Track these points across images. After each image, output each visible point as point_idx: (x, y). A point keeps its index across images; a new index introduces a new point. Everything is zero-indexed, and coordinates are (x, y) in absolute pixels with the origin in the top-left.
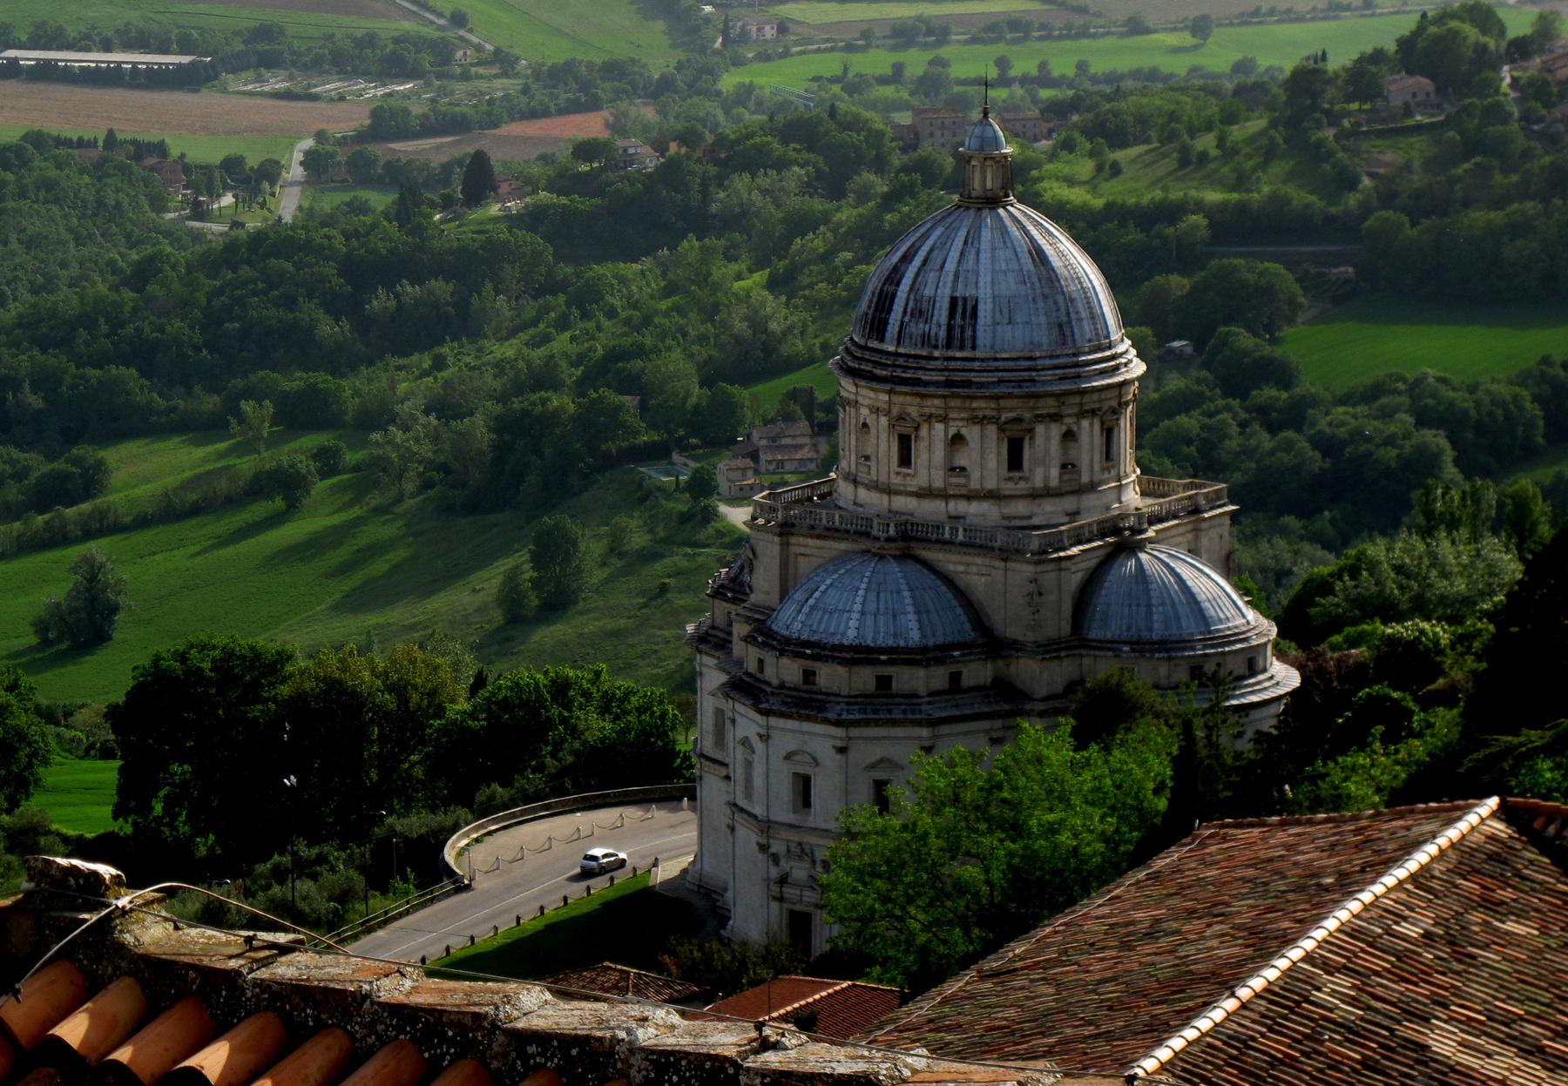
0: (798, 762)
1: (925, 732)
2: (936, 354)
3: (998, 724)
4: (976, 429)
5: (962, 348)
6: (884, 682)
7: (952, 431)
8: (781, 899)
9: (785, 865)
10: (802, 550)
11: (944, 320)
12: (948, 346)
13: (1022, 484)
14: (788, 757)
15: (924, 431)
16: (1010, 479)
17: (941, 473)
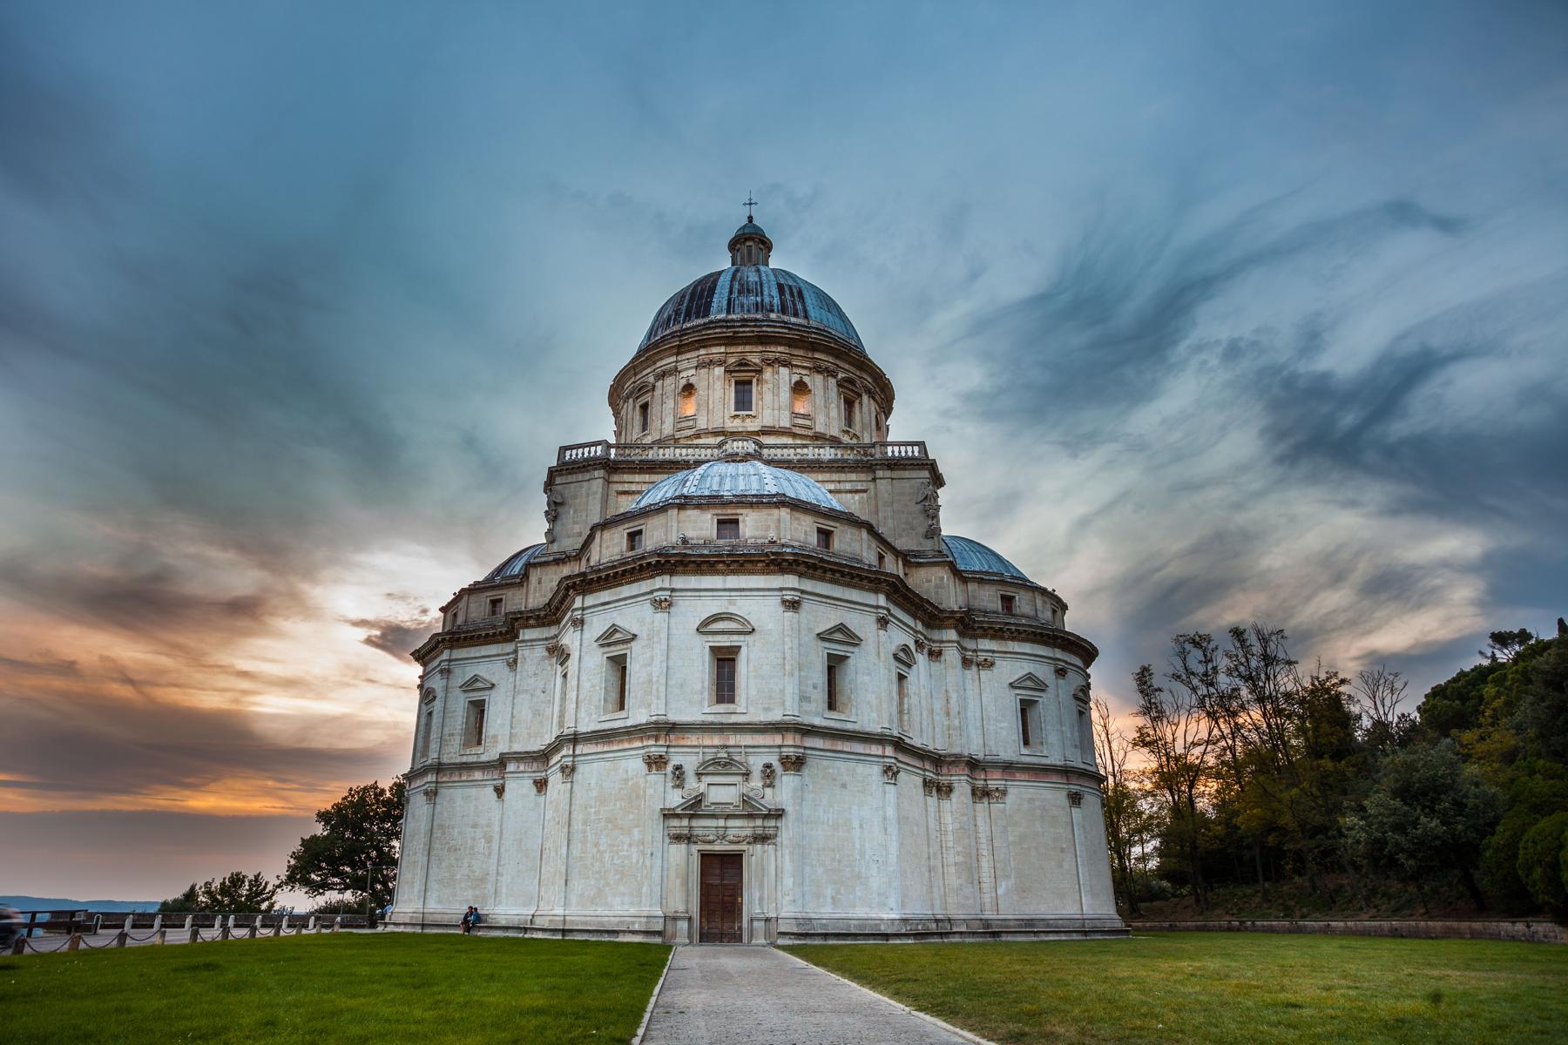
1: (882, 600)
2: (773, 316)
3: (920, 627)
4: (819, 378)
5: (796, 315)
6: (825, 535)
7: (795, 378)
8: (688, 839)
9: (693, 785)
10: (626, 487)
11: (775, 292)
12: (784, 310)
14: (703, 628)
15: (768, 374)
17: (787, 413)
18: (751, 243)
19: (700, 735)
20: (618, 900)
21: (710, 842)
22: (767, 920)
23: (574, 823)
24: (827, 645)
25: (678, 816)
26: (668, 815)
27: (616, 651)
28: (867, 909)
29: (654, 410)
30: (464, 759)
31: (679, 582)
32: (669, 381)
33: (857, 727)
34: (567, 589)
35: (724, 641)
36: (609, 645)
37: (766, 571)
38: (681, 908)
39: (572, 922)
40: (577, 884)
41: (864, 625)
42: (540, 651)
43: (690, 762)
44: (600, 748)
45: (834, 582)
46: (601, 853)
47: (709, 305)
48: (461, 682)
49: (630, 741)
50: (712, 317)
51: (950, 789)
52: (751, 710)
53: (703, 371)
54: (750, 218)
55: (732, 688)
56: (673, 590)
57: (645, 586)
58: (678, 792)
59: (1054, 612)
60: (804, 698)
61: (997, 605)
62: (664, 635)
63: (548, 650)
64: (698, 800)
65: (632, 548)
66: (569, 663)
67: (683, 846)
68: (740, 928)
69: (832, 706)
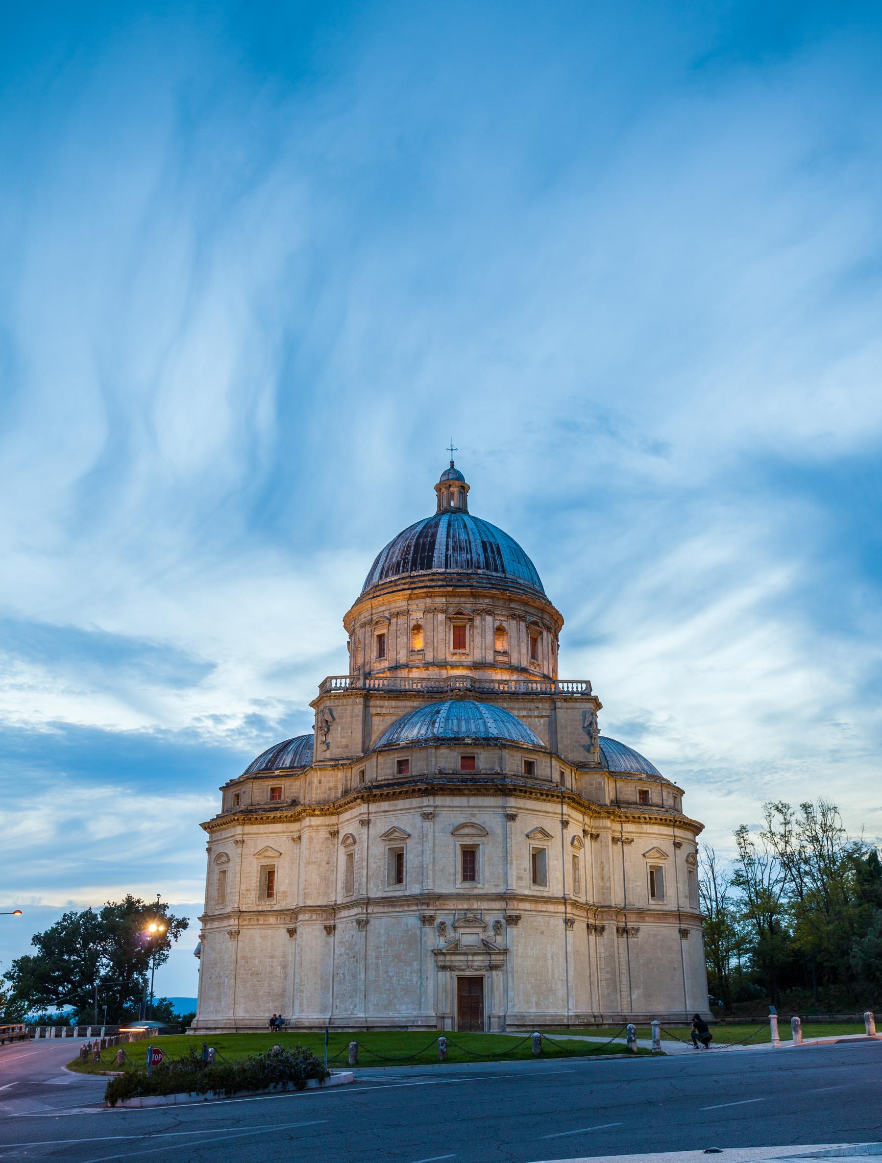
0: (468, 835)
2: (480, 571)
3: (587, 820)
5: (496, 570)
6: (530, 766)
7: (497, 623)
8: (451, 968)
10: (378, 710)
11: (480, 550)
12: (487, 567)
13: (537, 669)
15: (477, 621)
16: (533, 664)
18: (453, 485)
19: (455, 902)
20: (404, 1007)
21: (463, 970)
22: (499, 1017)
23: (369, 958)
24: (532, 842)
25: (444, 954)
26: (437, 953)
27: (396, 845)
28: (555, 1010)
29: (389, 643)
30: (260, 909)
31: (439, 800)
32: (402, 620)
33: (549, 894)
34: (355, 799)
35: (469, 841)
36: (390, 840)
37: (495, 795)
38: (448, 1011)
39: (372, 1022)
40: (373, 998)
41: (553, 826)
42: (323, 834)
43: (449, 920)
44: (386, 909)
45: (536, 799)
46: (391, 978)
47: (430, 558)
48: (253, 851)
49: (409, 905)
50: (434, 570)
51: (603, 929)
52: (487, 886)
53: (430, 616)
54: (452, 463)
55: (473, 870)
56: (436, 807)
57: (415, 802)
58: (442, 939)
59: (675, 798)
60: (520, 878)
61: (636, 798)
62: (430, 837)
63: (330, 833)
64: (457, 944)
65: (400, 771)
66: (356, 847)
67: (448, 973)
68: (482, 1023)
69: (535, 881)
